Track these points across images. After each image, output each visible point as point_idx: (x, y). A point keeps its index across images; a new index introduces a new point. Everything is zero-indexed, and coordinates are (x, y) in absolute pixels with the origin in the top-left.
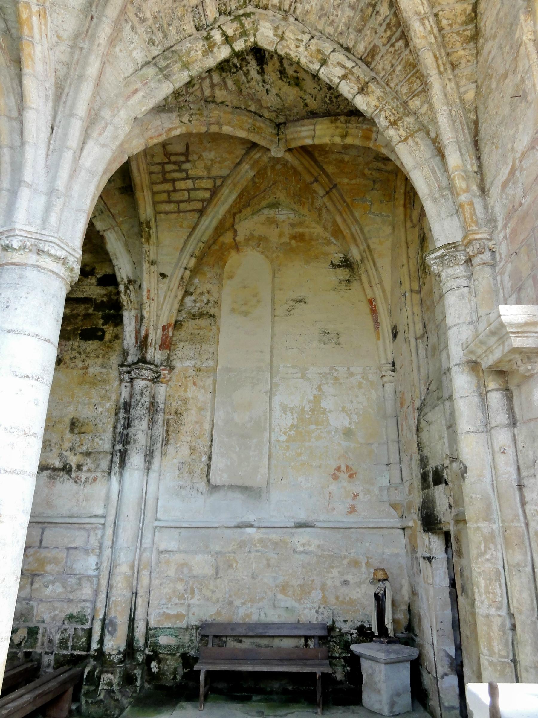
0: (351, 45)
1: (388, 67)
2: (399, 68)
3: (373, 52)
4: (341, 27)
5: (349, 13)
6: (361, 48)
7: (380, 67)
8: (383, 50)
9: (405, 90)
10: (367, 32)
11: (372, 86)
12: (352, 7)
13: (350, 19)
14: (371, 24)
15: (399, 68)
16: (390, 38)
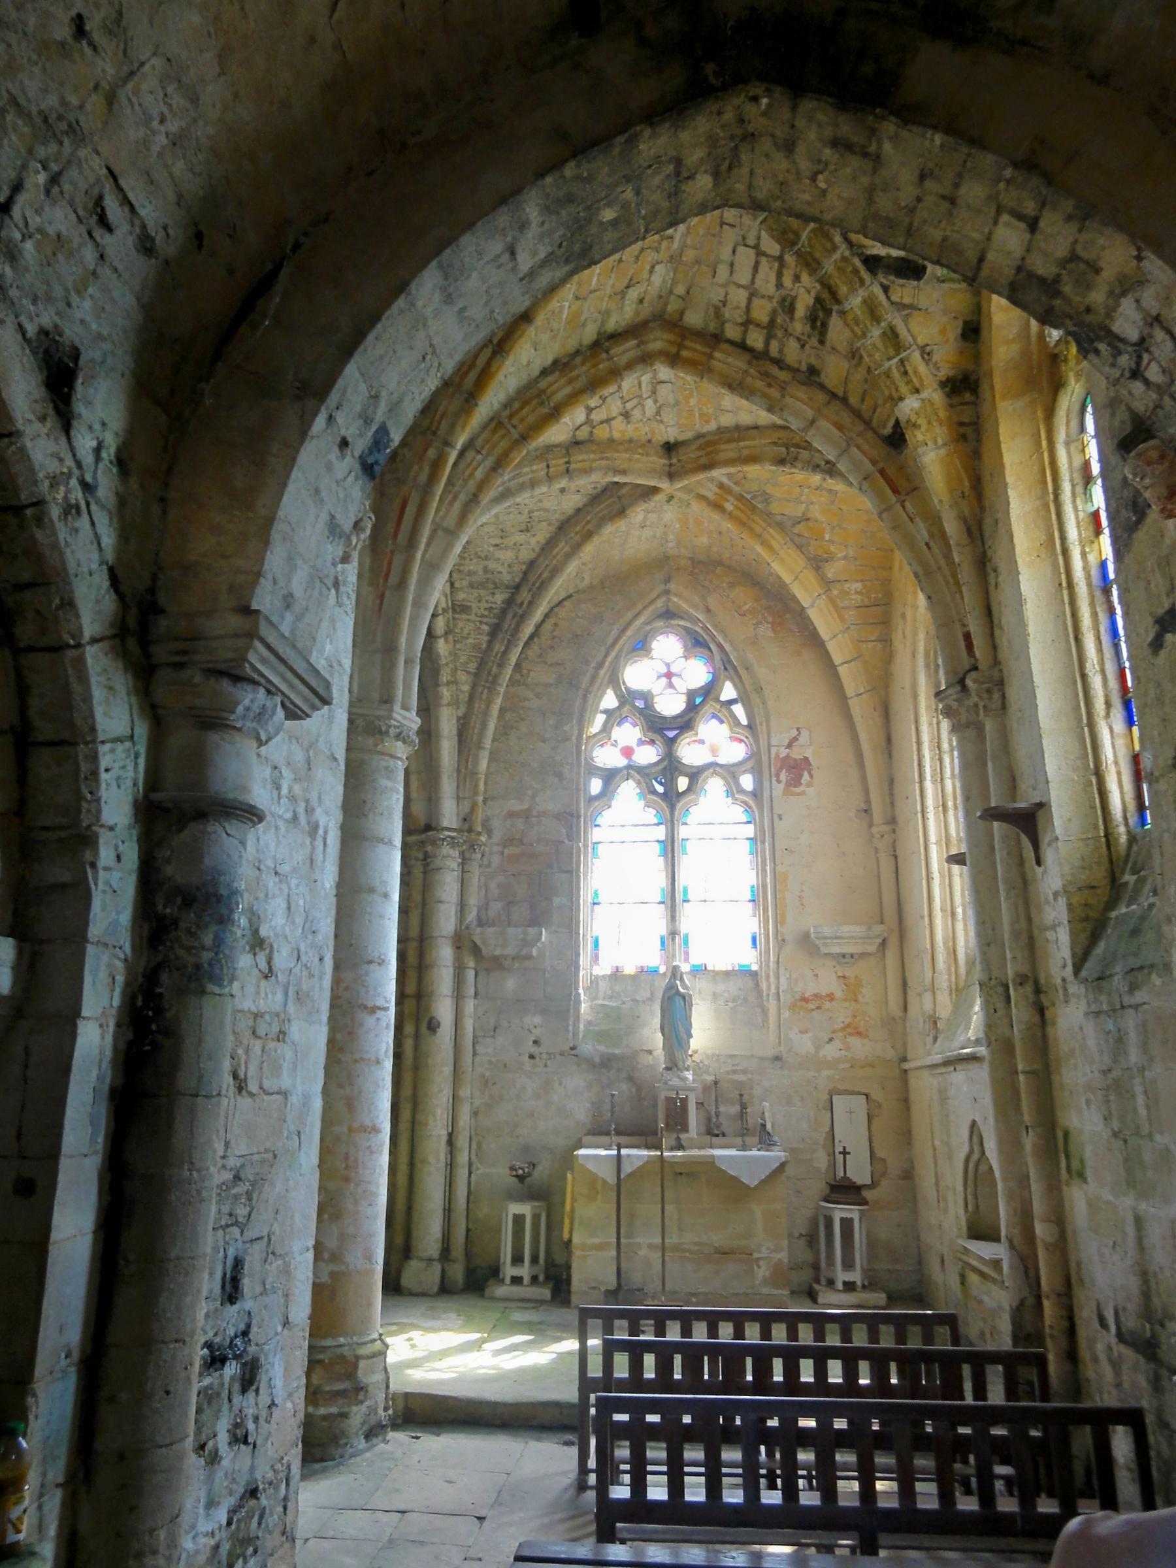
0: (457, 585)
1: (466, 631)
2: (471, 641)
3: (465, 609)
4: (465, 569)
5: (480, 568)
6: (461, 596)
7: (460, 624)
8: (473, 617)
9: (463, 659)
10: (476, 593)
11: (450, 638)
12: (486, 570)
13: (475, 573)
14: (482, 592)
15: (471, 641)
16: (482, 616)
